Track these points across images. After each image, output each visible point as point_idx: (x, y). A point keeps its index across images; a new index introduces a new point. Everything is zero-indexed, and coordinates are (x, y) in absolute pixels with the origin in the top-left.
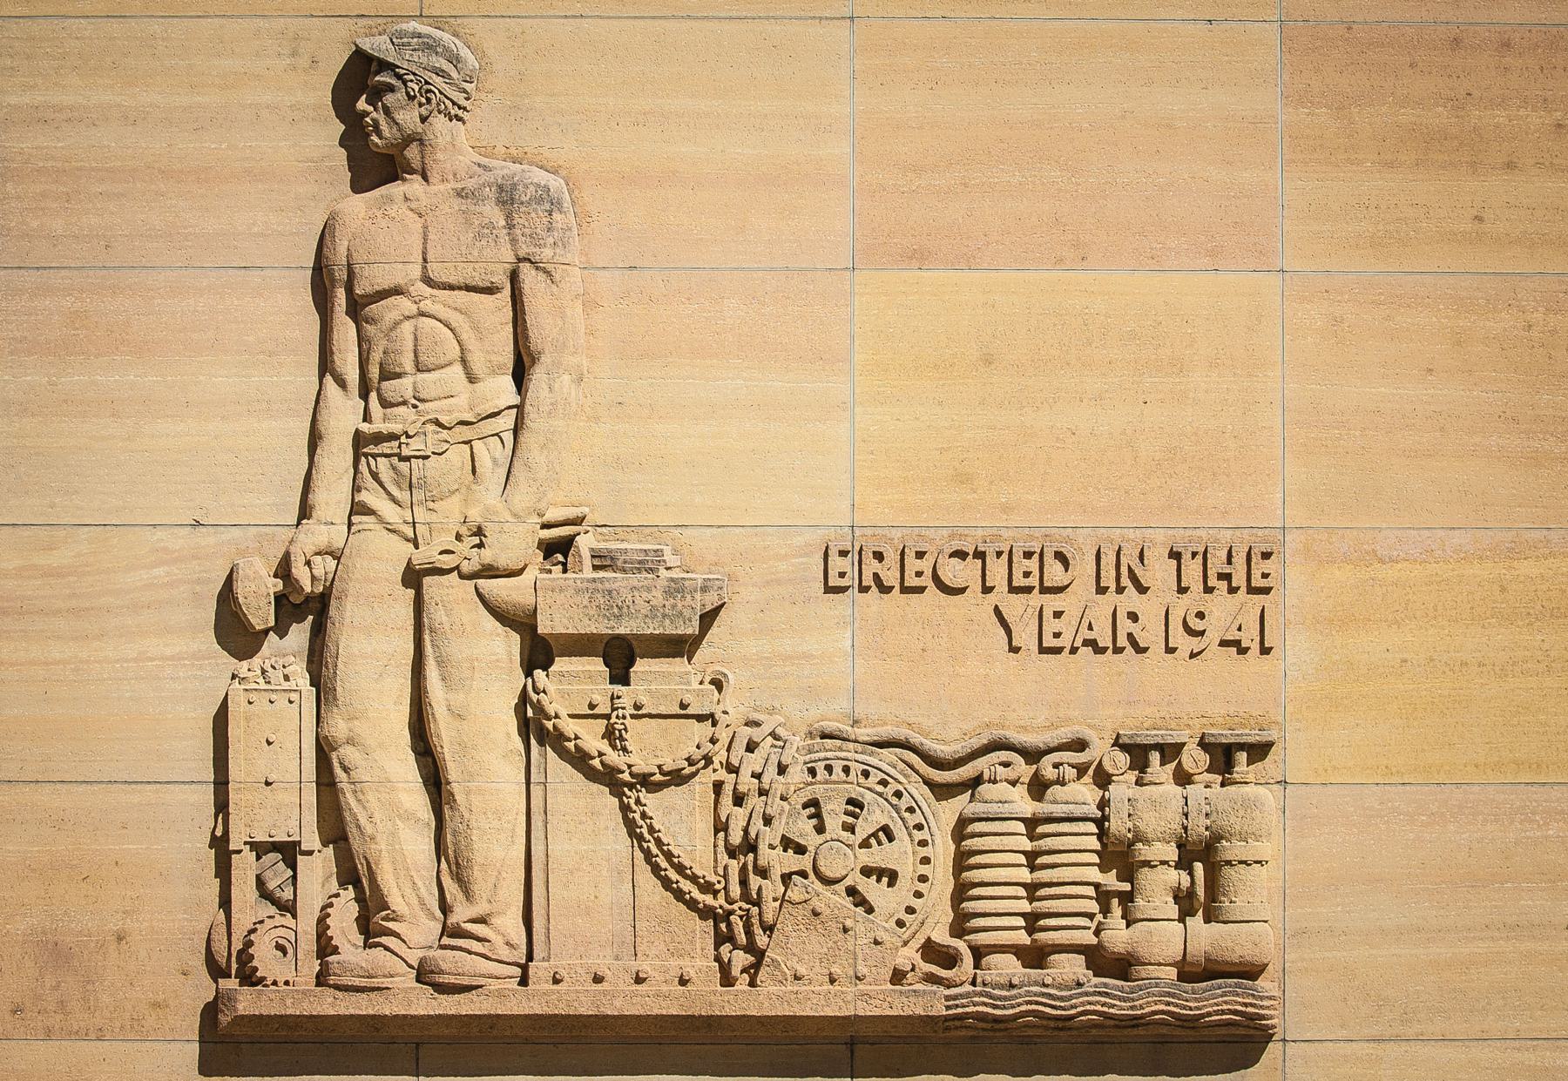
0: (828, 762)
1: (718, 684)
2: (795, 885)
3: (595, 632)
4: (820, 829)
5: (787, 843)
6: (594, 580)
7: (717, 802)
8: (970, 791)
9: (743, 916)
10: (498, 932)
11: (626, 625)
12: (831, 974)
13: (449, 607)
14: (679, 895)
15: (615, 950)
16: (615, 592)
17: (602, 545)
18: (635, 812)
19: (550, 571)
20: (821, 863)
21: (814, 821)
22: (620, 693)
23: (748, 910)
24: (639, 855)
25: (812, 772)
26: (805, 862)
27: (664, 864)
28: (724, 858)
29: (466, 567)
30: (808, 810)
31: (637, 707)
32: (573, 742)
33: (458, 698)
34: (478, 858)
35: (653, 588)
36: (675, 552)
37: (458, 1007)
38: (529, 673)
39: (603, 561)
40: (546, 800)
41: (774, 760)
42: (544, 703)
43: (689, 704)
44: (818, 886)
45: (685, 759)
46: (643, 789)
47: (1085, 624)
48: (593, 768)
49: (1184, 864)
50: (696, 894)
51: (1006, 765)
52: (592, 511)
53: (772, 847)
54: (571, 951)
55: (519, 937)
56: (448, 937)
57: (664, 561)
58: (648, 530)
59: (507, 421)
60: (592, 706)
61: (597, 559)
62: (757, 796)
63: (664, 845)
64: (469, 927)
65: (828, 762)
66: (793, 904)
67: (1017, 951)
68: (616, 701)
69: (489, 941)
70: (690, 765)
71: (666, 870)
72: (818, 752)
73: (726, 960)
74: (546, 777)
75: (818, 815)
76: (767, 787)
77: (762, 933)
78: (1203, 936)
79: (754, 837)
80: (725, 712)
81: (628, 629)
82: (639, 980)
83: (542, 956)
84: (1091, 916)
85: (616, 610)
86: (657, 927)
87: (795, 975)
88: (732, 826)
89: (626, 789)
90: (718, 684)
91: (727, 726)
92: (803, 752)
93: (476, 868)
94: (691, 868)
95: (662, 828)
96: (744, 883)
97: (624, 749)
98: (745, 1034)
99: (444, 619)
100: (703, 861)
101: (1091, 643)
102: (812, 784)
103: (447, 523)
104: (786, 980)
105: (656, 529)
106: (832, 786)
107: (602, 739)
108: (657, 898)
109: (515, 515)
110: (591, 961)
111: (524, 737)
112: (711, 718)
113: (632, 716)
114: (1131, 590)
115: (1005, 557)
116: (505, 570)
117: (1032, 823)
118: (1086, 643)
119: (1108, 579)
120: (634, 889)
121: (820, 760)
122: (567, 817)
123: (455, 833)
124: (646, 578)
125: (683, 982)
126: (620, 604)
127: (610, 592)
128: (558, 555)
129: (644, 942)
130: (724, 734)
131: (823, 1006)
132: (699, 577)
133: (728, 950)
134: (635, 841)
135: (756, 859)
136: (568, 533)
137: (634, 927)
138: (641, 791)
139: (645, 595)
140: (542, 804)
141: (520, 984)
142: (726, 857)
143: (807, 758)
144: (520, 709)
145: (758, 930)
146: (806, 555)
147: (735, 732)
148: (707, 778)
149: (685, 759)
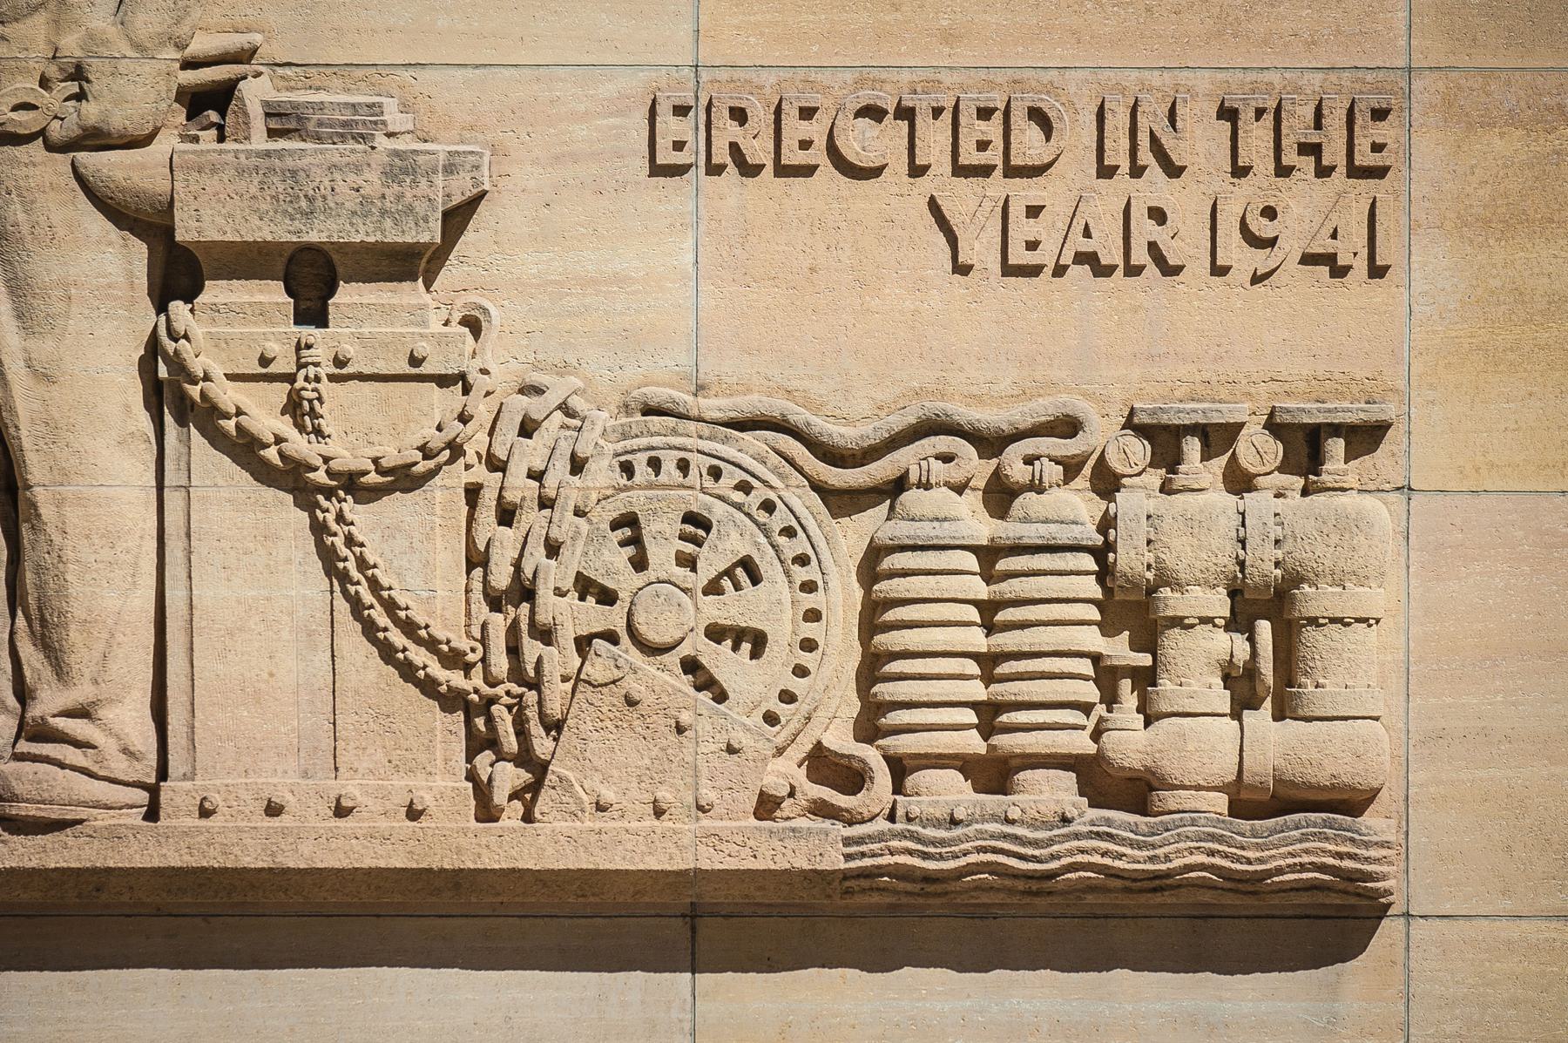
0: (653, 453)
1: (473, 325)
2: (596, 654)
3: (269, 238)
4: (640, 564)
5: (585, 586)
6: (268, 154)
7: (471, 519)
8: (888, 502)
9: (515, 705)
10: (110, 732)
11: (322, 227)
12: (655, 800)
13: (29, 197)
14: (407, 671)
15: (302, 761)
16: (302, 174)
17: (285, 96)
18: (335, 534)
19: (196, 139)
20: (640, 619)
21: (630, 551)
22: (311, 340)
23: (521, 696)
24: (342, 606)
25: (628, 469)
26: (614, 618)
27: (382, 619)
28: (481, 610)
29: (56, 131)
30: (619, 532)
31: (339, 362)
32: (234, 420)
33: (43, 347)
34: (77, 610)
35: (365, 167)
36: (405, 108)
37: (42, 855)
38: (161, 308)
39: (284, 121)
40: (189, 515)
41: (565, 449)
42: (185, 355)
43: (424, 358)
44: (635, 656)
45: (418, 448)
46: (349, 498)
47: (1078, 228)
48: (265, 463)
49: (1240, 622)
50: (436, 670)
51: (947, 458)
52: (268, 40)
53: (559, 593)
54: (230, 763)
55: (143, 736)
56: (27, 740)
57: (384, 123)
58: (359, 73)
60: (264, 361)
61: (274, 119)
62: (537, 508)
63: (382, 589)
64: (62, 723)
65: (653, 453)
66: (594, 686)
67: (965, 764)
68: (304, 352)
69: (94, 747)
70: (426, 457)
71: (385, 630)
72: (637, 436)
73: (485, 778)
74: (189, 477)
75: (636, 541)
76: (552, 494)
77: (543, 734)
79: (530, 576)
80: (484, 372)
81: (324, 234)
82: (341, 811)
83: (182, 771)
84: (1086, 708)
85: (304, 204)
86: (371, 723)
87: (597, 803)
88: (495, 555)
89: (320, 498)
90: (473, 325)
91: (488, 394)
92: (613, 437)
93: (73, 627)
94: (427, 627)
95: (380, 562)
96: (514, 651)
97: (318, 432)
98: (517, 899)
99: (21, 217)
100: (448, 614)
101: (1087, 259)
102: (626, 489)
103: (26, 59)
104: (583, 811)
105: (373, 70)
106: (660, 492)
107: (282, 414)
108: (371, 676)
109: (137, 46)
110: (264, 780)
111: (154, 410)
112: (460, 381)
113: (332, 378)
114: (1155, 171)
115: (947, 117)
116: (121, 137)
117: (988, 555)
118: (1081, 258)
119: (1117, 153)
120: (333, 661)
121: (640, 450)
122: (223, 544)
123: (39, 570)
124: (353, 151)
125: (413, 814)
126: (311, 192)
127: (294, 173)
128: (210, 111)
129: (350, 748)
130: (481, 407)
131: (643, 854)
132: (441, 149)
133: (488, 761)
134: (335, 583)
135: (533, 612)
136: (226, 76)
137: (334, 724)
138: (345, 500)
139: (351, 177)
140: (182, 522)
141: (147, 817)
142: (486, 609)
143: (620, 447)
144: (147, 365)
145: (536, 729)
146: (619, 113)
147: (502, 404)
148: (455, 478)
149: (418, 448)
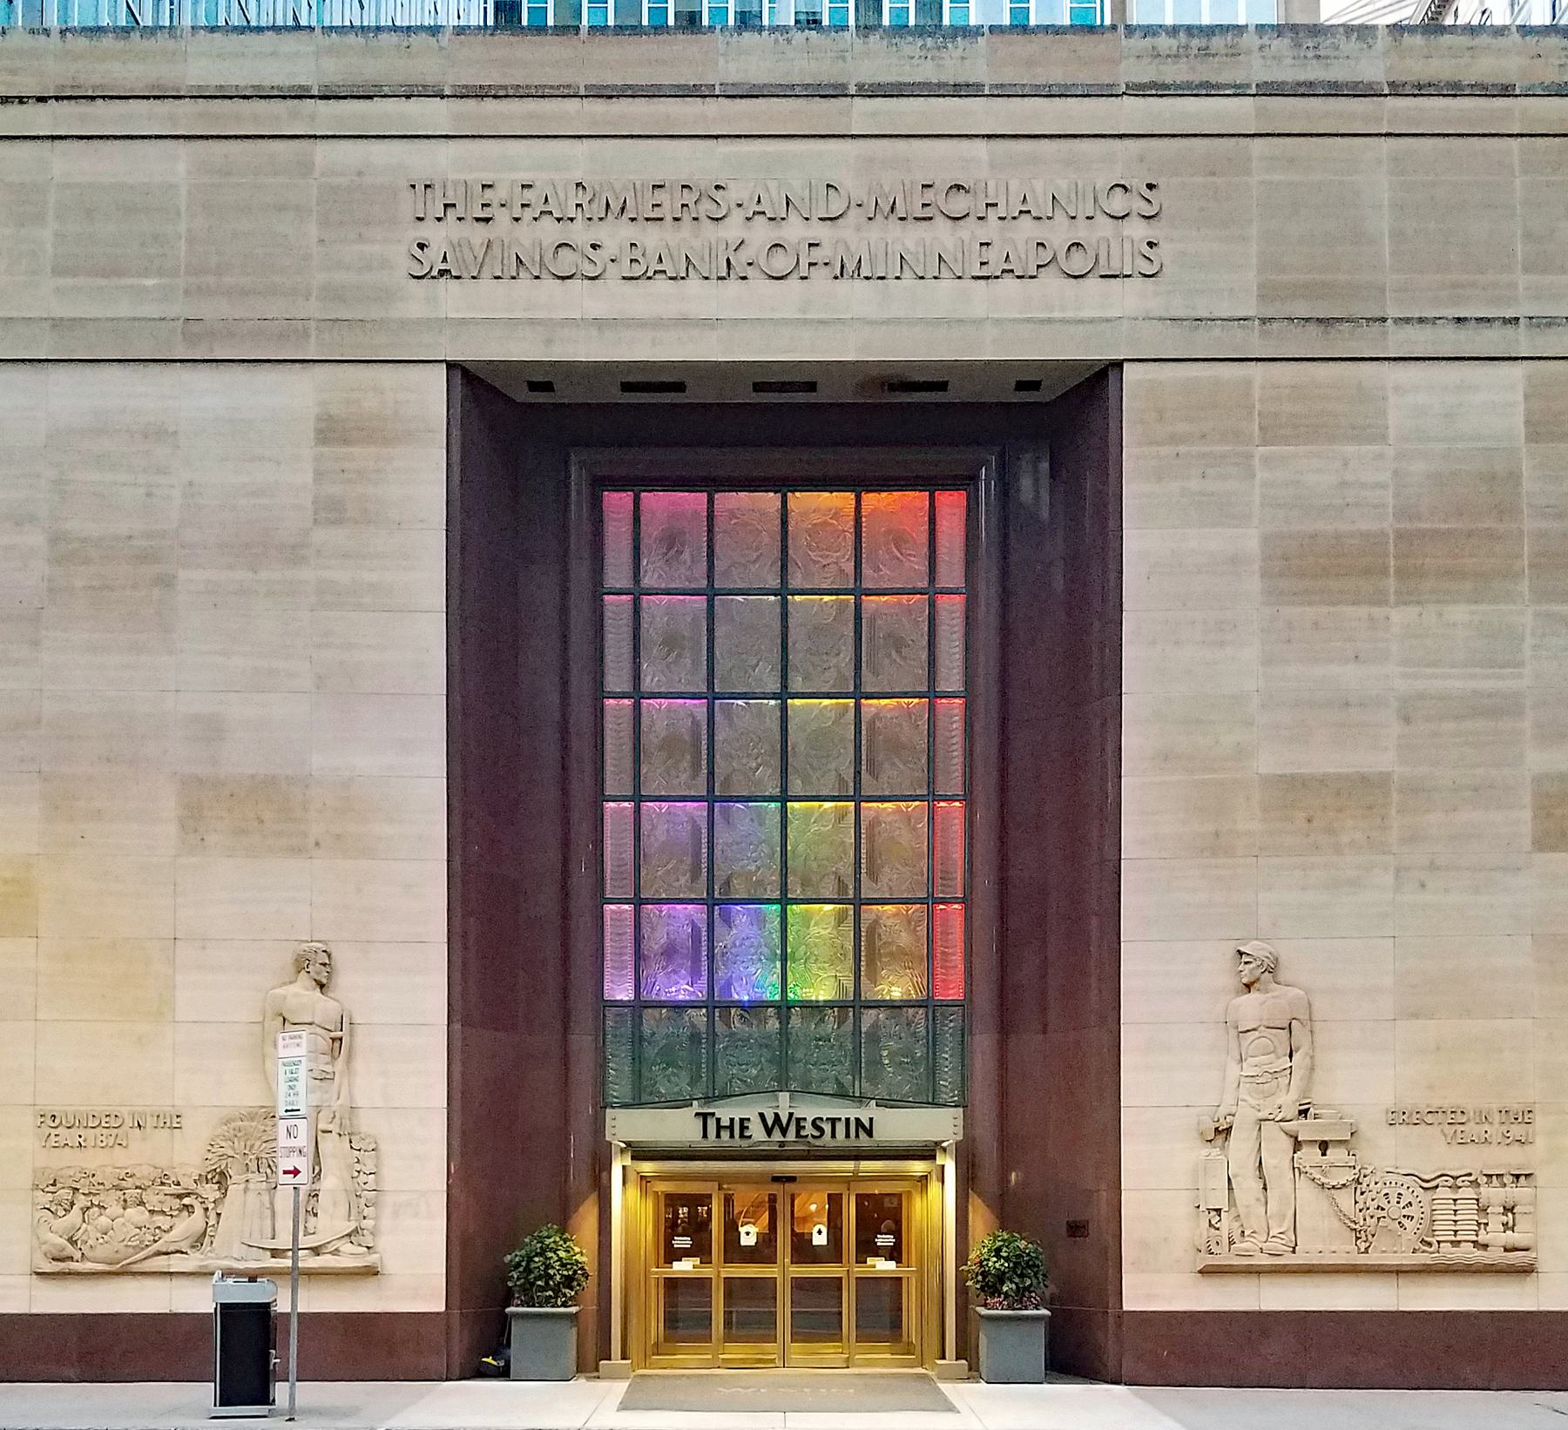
51: (1447, 1181)
59: (1289, 1071)
78: (1511, 1238)
84: (1475, 1231)
